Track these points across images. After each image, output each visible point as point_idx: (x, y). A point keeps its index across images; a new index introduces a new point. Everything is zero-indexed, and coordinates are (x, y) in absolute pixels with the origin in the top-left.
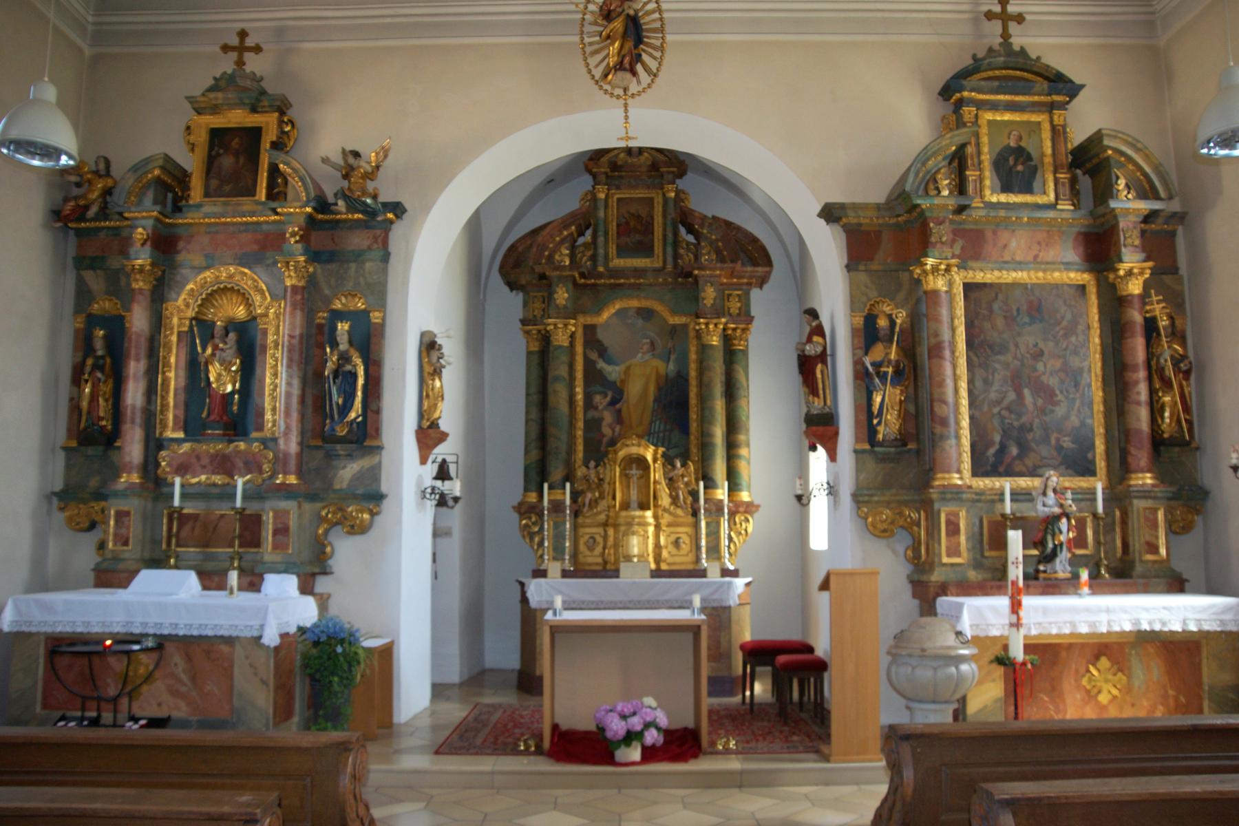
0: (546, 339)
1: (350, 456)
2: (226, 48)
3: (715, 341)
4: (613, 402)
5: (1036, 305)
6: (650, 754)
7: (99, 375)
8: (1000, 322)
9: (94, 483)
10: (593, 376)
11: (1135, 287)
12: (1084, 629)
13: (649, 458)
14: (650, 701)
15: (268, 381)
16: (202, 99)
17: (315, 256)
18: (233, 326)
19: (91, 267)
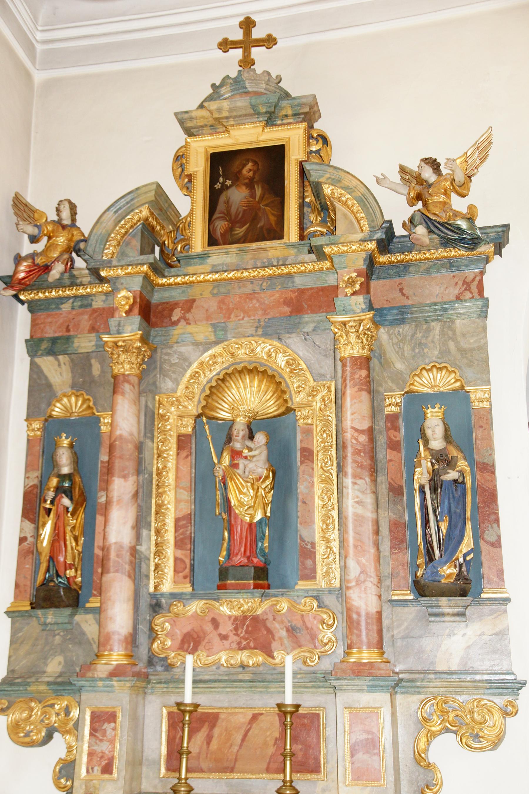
2: (226, 45)
7: (66, 501)
9: (54, 667)
15: (318, 502)
16: (203, 113)
17: (380, 315)
19: (51, 352)
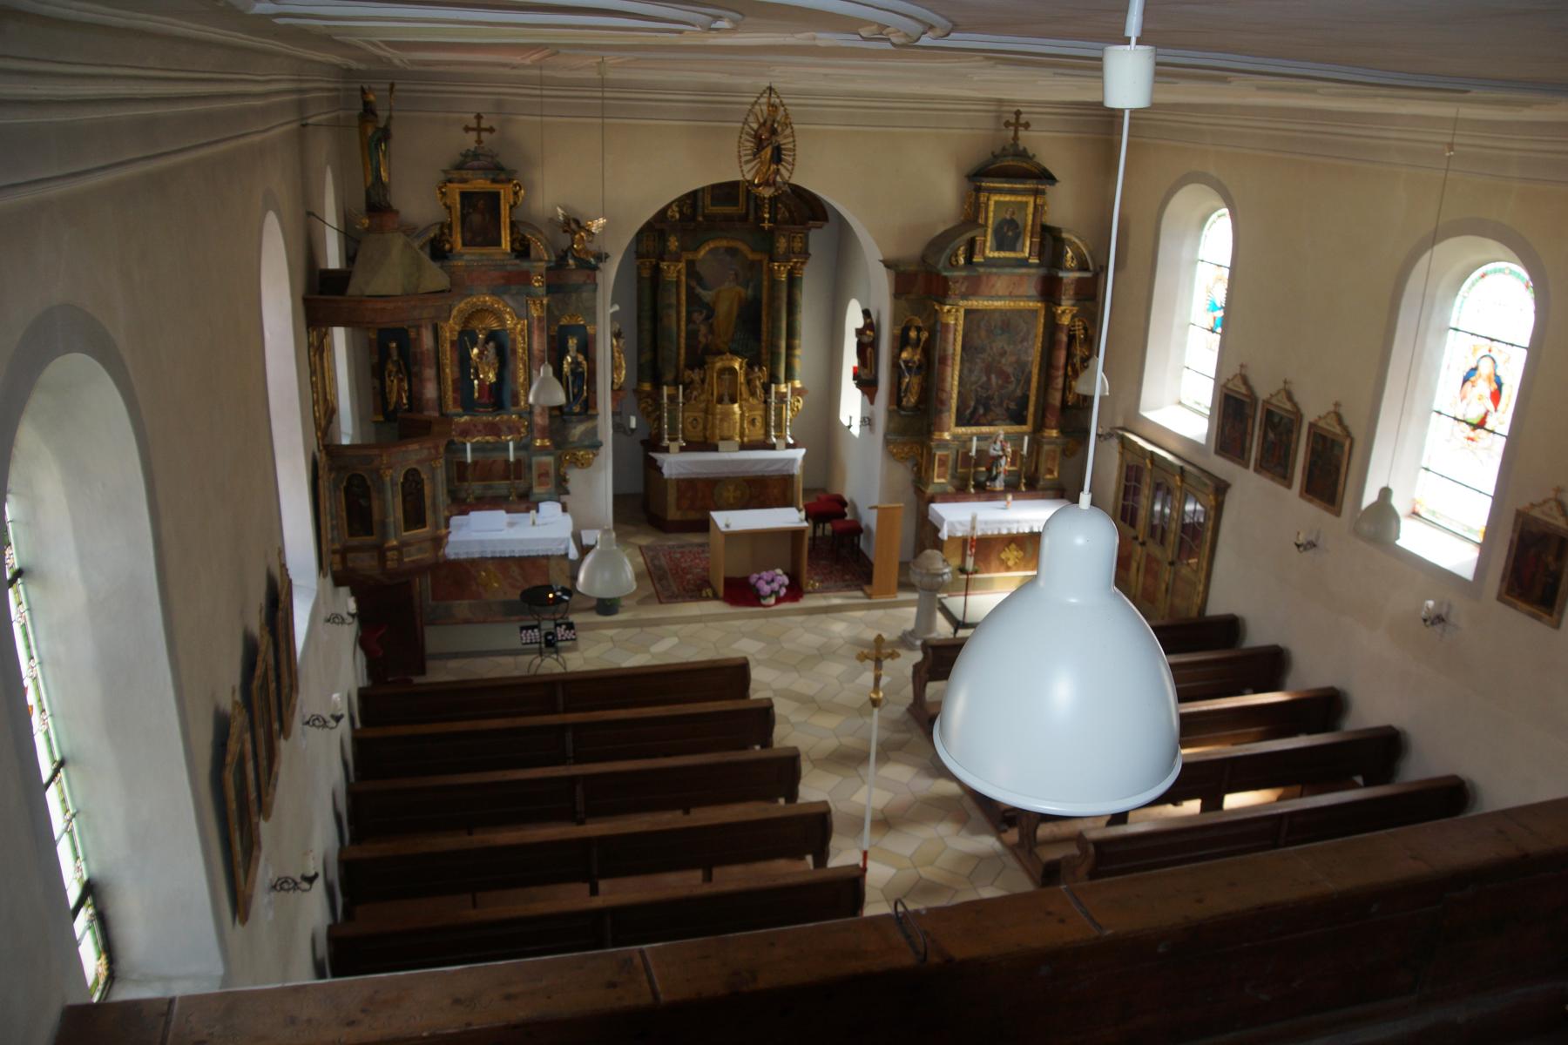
0: (656, 270)
1: (581, 422)
3: (784, 277)
4: (708, 318)
5: (1007, 323)
6: (779, 600)
8: (983, 333)
10: (693, 299)
11: (1066, 320)
12: (1004, 532)
13: (737, 366)
14: (779, 571)
18: (492, 336)
